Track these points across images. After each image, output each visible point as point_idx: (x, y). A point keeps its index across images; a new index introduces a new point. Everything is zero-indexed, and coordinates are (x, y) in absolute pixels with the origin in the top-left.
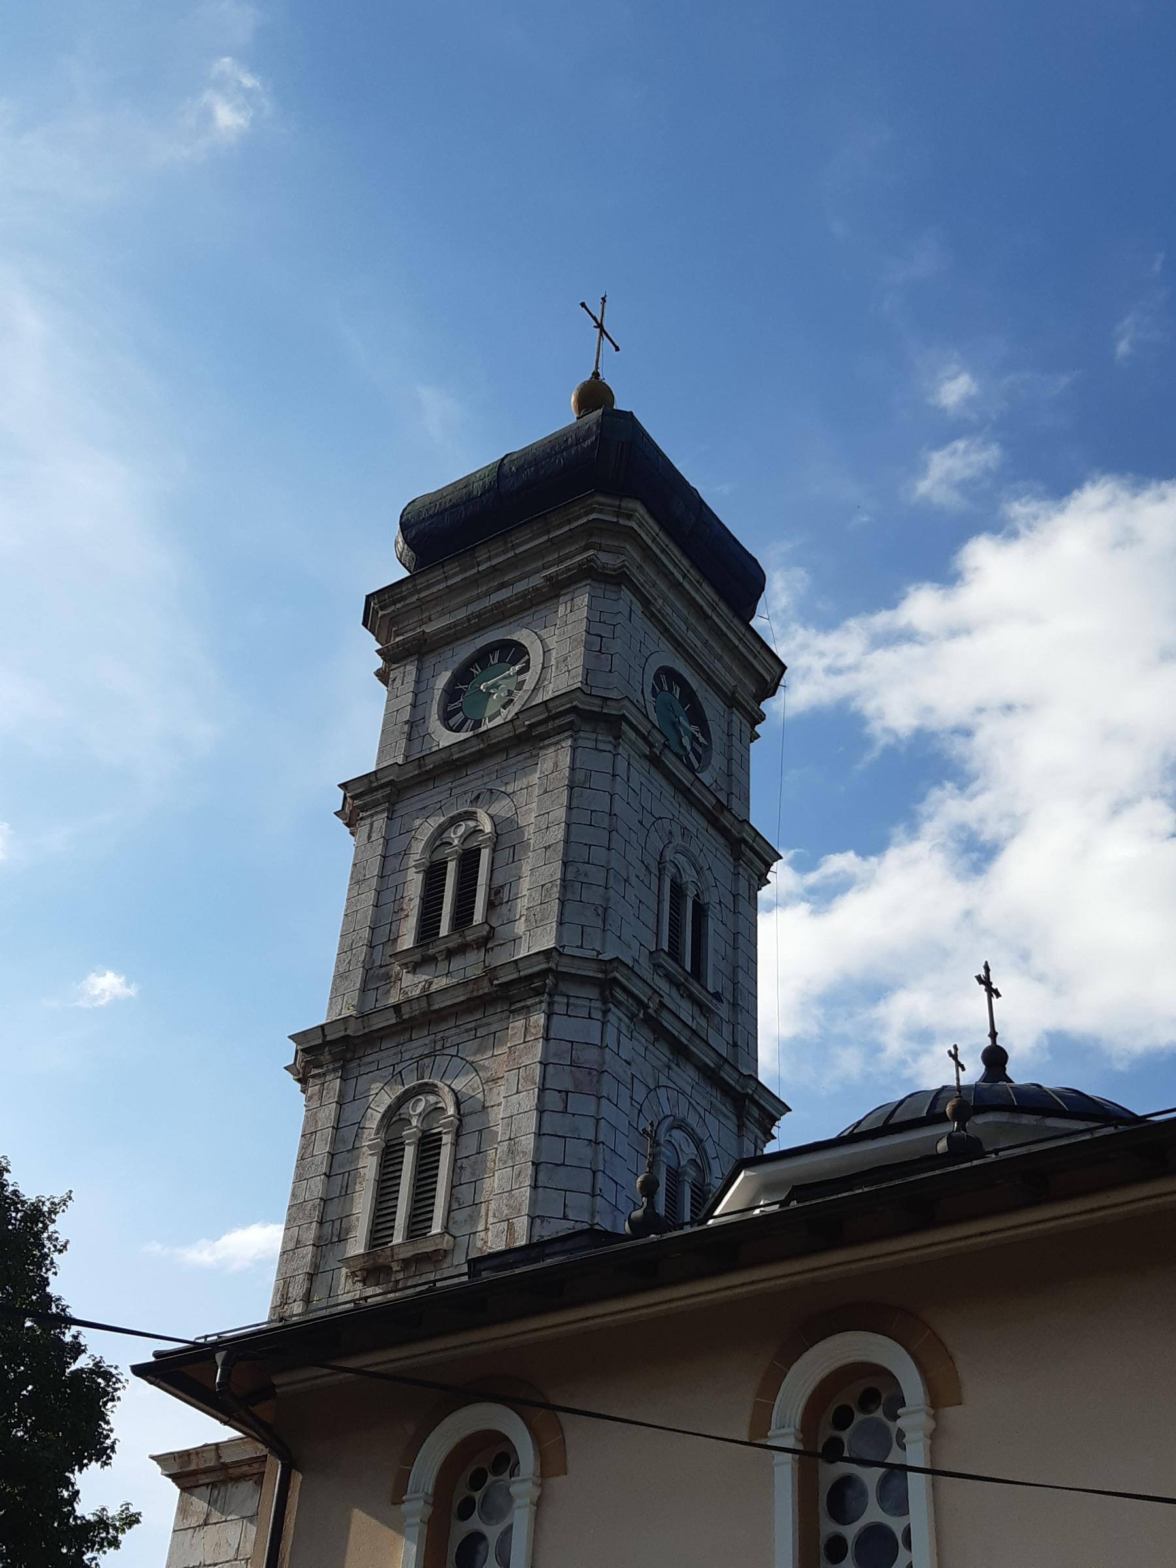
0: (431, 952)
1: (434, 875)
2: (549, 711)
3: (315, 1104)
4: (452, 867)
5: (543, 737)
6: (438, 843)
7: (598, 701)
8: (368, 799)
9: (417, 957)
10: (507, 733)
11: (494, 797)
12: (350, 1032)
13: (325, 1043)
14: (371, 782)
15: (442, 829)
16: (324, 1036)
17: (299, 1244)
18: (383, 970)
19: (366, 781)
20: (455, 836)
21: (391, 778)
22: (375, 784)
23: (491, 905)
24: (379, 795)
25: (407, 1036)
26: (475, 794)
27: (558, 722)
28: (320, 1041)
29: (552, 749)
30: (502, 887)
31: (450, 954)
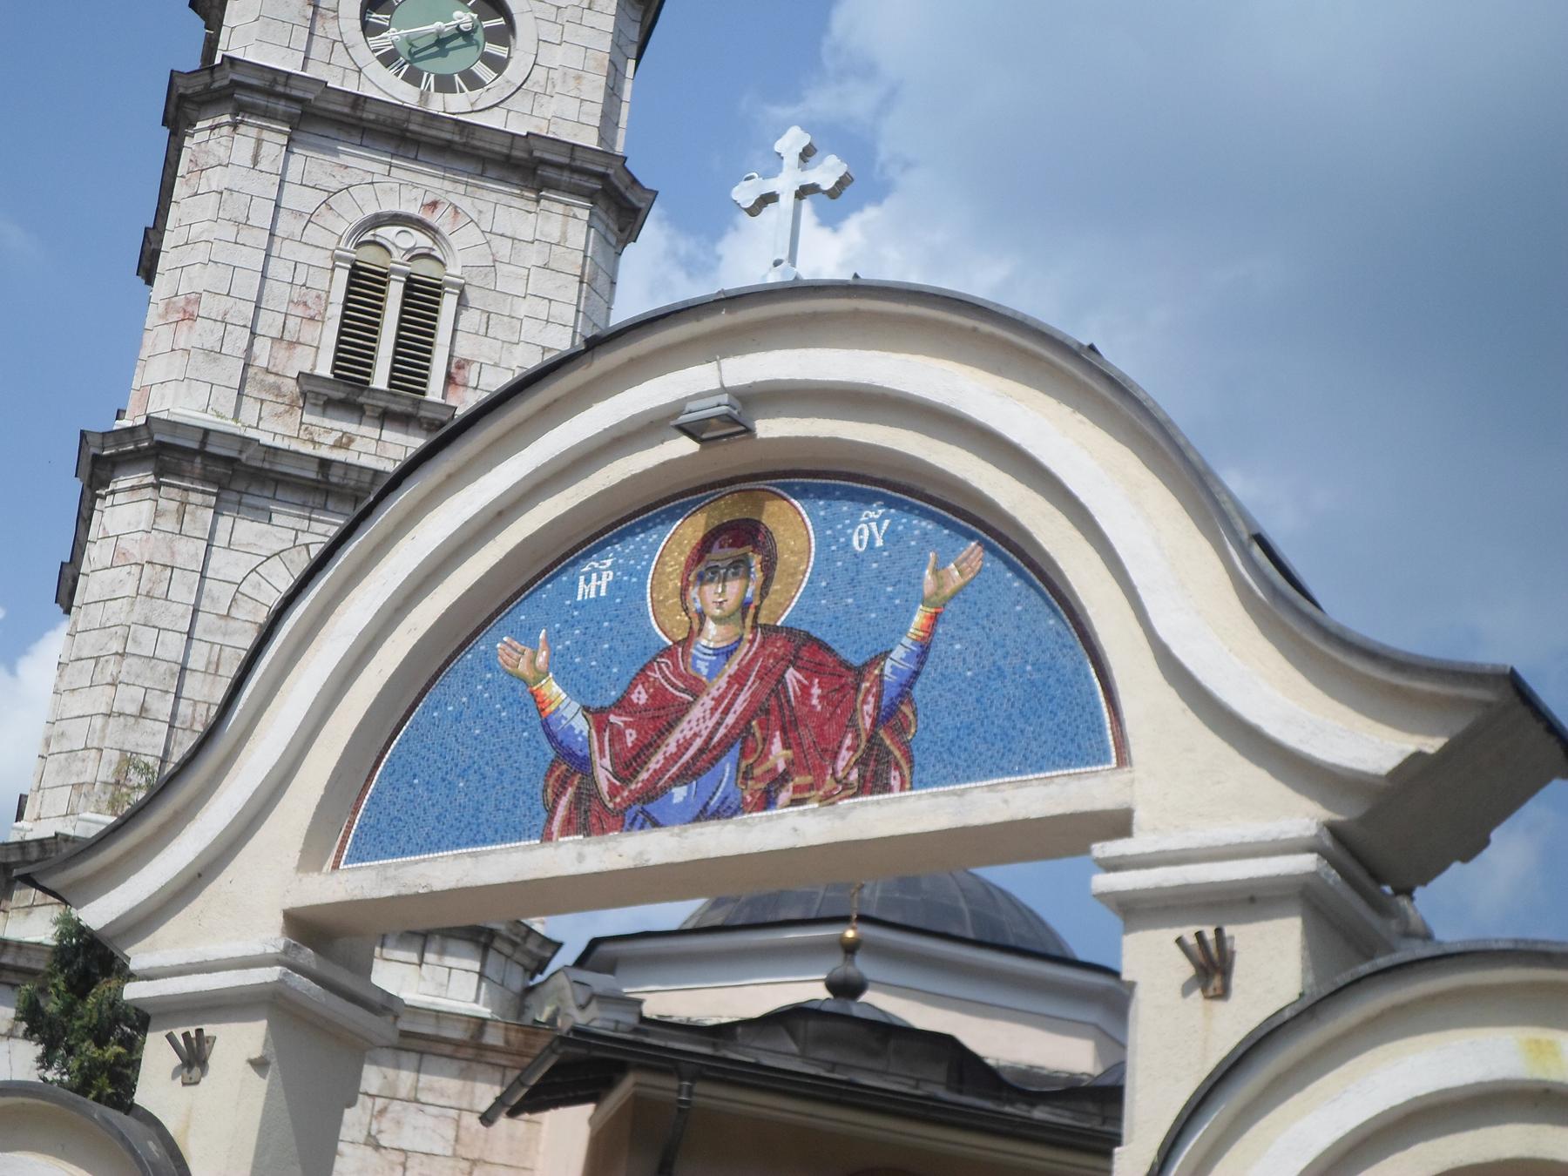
0: (361, 399)
1: (364, 285)
2: (572, 159)
3: (168, 524)
4: (395, 292)
5: (555, 186)
6: (368, 236)
7: (627, 180)
8: (260, 100)
9: (339, 394)
10: (500, 147)
11: (463, 220)
12: (243, 457)
13: (201, 452)
14: (275, 81)
15: (378, 221)
16: (204, 442)
17: (143, 713)
18: (271, 379)
19: (269, 76)
20: (401, 240)
21: (311, 96)
22: (280, 89)
23: (450, 379)
24: (281, 106)
25: (319, 500)
26: (428, 200)
27: (576, 178)
28: (195, 446)
29: (559, 208)
30: (468, 361)
31: (386, 418)
